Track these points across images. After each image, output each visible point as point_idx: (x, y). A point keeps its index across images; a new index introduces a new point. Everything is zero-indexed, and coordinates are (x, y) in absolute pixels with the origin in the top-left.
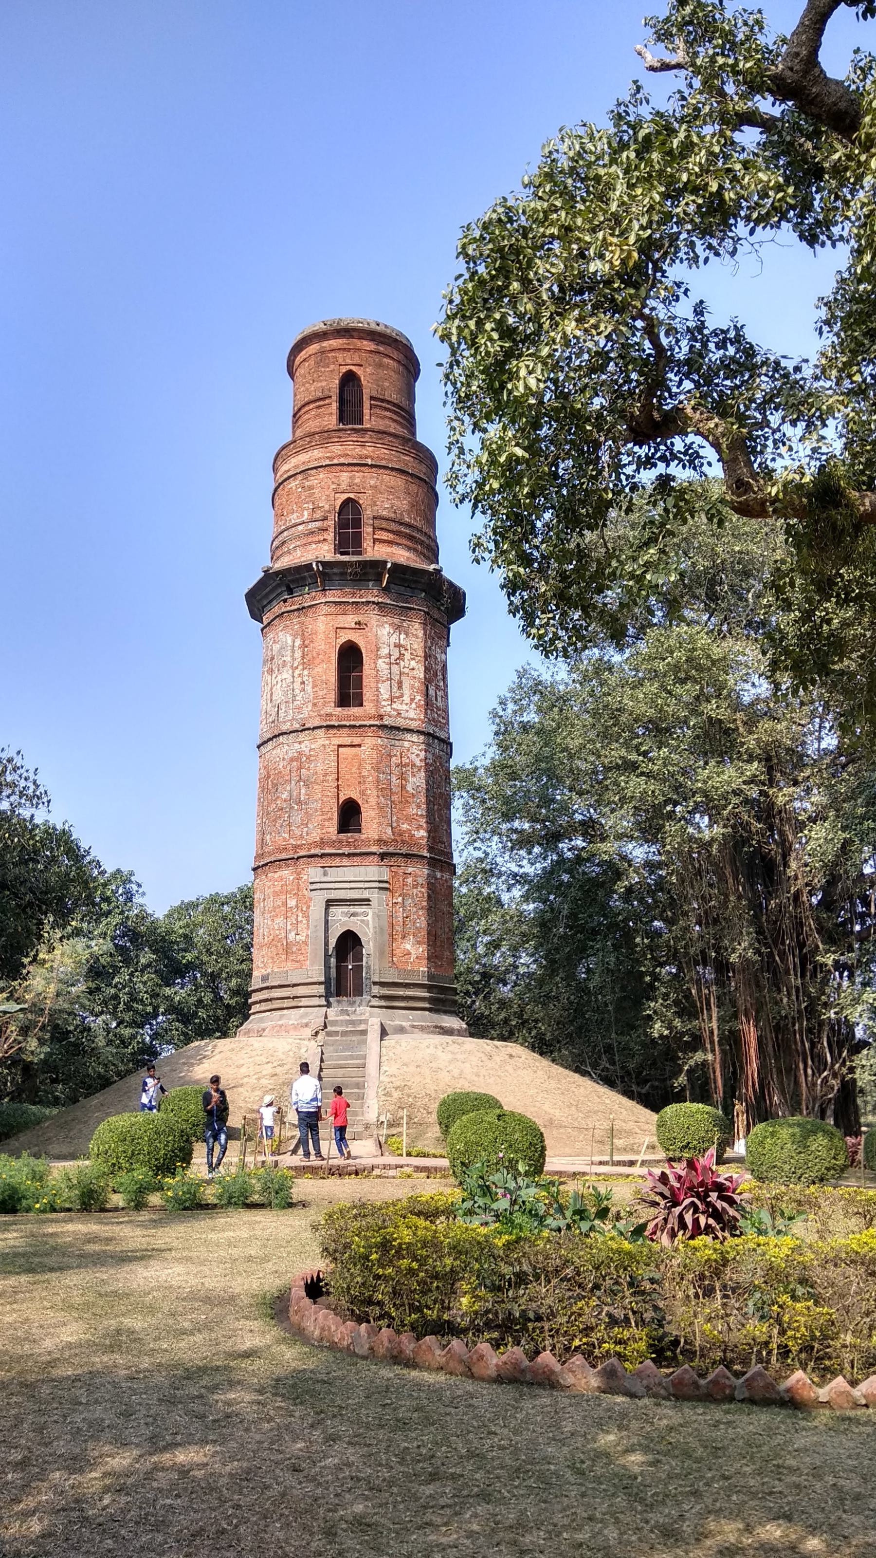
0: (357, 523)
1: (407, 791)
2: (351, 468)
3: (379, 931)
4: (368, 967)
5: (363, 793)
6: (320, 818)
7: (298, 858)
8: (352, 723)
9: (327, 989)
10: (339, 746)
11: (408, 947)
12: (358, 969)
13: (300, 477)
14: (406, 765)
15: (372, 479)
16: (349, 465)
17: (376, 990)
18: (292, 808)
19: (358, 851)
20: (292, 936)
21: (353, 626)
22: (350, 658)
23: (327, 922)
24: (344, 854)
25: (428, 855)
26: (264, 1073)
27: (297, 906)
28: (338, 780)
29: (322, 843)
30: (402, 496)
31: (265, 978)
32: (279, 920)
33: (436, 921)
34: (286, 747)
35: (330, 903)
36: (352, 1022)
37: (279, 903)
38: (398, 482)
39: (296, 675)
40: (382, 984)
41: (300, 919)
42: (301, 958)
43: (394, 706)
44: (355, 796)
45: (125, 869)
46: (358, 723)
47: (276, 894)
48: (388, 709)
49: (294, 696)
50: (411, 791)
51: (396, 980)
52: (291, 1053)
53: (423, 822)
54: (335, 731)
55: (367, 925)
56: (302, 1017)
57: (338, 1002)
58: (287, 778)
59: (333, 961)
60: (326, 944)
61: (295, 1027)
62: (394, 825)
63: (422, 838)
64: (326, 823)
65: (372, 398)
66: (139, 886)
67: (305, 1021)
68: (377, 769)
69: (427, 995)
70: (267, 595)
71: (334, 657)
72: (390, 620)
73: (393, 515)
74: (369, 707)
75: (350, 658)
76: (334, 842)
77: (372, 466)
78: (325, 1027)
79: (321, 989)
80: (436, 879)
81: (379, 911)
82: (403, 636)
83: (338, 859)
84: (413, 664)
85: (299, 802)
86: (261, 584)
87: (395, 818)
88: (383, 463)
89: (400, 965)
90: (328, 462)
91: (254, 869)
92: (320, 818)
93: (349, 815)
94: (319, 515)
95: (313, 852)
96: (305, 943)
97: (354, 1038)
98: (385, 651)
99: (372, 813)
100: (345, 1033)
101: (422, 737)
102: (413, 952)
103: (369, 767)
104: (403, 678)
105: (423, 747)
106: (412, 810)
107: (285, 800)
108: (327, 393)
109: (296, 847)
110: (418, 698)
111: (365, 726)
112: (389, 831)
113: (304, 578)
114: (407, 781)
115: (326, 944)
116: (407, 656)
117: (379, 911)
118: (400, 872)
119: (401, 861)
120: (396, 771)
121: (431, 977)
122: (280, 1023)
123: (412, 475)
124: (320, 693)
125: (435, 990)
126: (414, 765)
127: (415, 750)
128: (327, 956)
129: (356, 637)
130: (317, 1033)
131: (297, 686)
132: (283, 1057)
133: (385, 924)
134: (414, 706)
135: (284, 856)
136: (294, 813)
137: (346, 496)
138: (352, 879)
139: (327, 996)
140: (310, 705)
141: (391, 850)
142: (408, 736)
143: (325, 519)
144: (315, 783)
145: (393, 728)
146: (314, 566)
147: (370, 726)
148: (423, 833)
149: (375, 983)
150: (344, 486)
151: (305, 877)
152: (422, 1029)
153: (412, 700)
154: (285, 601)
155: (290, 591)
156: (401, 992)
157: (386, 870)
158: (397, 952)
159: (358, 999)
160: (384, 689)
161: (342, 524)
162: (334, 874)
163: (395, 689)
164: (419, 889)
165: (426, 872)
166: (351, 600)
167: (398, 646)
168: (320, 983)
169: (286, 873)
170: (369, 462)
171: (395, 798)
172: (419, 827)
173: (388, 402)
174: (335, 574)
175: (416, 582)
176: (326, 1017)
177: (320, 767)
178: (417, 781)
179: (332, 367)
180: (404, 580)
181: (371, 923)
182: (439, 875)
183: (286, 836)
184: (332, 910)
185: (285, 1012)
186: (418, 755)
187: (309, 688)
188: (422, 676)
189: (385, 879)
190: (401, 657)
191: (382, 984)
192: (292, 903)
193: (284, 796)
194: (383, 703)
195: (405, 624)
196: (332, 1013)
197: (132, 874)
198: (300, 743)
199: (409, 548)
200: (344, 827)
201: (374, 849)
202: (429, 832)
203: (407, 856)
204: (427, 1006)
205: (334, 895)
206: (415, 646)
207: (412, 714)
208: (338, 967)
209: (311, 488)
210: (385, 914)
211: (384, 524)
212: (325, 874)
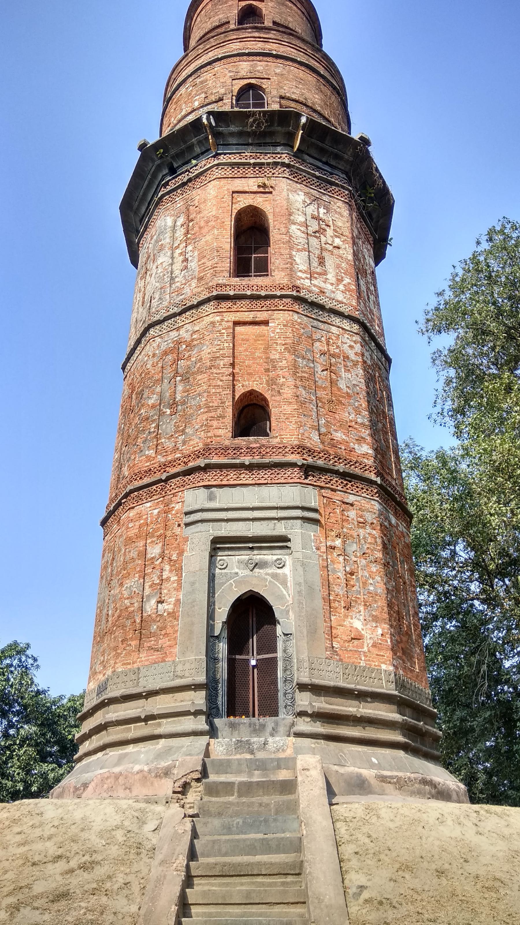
1: (339, 389)
2: (251, 58)
3: (306, 591)
4: (288, 659)
5: (272, 382)
6: (205, 416)
7: (168, 478)
9: (211, 699)
10: (236, 323)
11: (358, 624)
12: (268, 667)
13: (191, 79)
14: (333, 356)
15: (277, 68)
17: (305, 701)
18: (161, 414)
19: (267, 460)
20: (150, 606)
21: (255, 189)
22: (251, 235)
23: (212, 578)
24: (242, 466)
25: (378, 480)
26: (39, 888)
27: (162, 555)
28: (233, 365)
29: (207, 450)
31: (102, 688)
32: (132, 583)
33: (397, 589)
34: (158, 340)
35: (218, 544)
36: (262, 766)
37: (134, 554)
39: (176, 254)
40: (317, 690)
41: (165, 575)
42: (164, 642)
44: (258, 385)
45: (22, 641)
47: (130, 541)
48: (307, 283)
49: (172, 279)
50: (345, 389)
51: (341, 684)
52: (119, 836)
53: (366, 433)
54: (229, 304)
55: (284, 583)
56: (159, 756)
57: (233, 726)
58: (157, 377)
59: (222, 647)
60: (211, 616)
61: (144, 778)
62: (323, 430)
63: (365, 455)
64: (215, 423)
66: (35, 660)
67: (164, 764)
68: (293, 349)
69: (396, 717)
70: (145, 194)
71: (229, 224)
72: (307, 190)
75: (251, 235)
76: (227, 448)
78: (204, 773)
79: (199, 699)
80: (390, 524)
81: (305, 557)
82: (322, 211)
83: (232, 474)
84: (337, 242)
85: (174, 404)
86: (139, 174)
87: (323, 421)
89: (346, 656)
91: (104, 523)
92: (205, 416)
93: (251, 415)
94: (213, 98)
95: (191, 465)
96: (173, 615)
97: (265, 799)
99: (288, 409)
100: (247, 789)
101: (356, 327)
102: (366, 634)
104: (325, 254)
105: (357, 338)
106: (347, 414)
107: (153, 406)
109: (164, 466)
110: (347, 280)
111: (274, 297)
112: (315, 437)
113: (190, 148)
114: (339, 376)
115: (211, 616)
116: (330, 232)
117: (305, 557)
118: (338, 496)
119: (336, 482)
121: (400, 685)
122: (117, 770)
124: (209, 264)
125: (408, 711)
128: (211, 639)
129: (259, 201)
130: (185, 787)
131: (178, 266)
132: (97, 842)
133: (317, 580)
134: (341, 287)
135: (146, 480)
136: (165, 419)
137: (246, 82)
138: (257, 504)
139: (211, 713)
140: (194, 283)
141: (320, 463)
142: (337, 321)
143: (221, 99)
144: (200, 372)
145: (314, 305)
146: (205, 121)
147: (282, 297)
148: (365, 449)
149: (302, 687)
150: (243, 73)
151: (178, 507)
152: (400, 785)
153: (340, 281)
154: (167, 184)
156: (351, 708)
158: (338, 631)
159: (269, 721)
160: (300, 260)
162: (225, 498)
163: (315, 263)
164: (369, 530)
165: (377, 506)
168: (197, 687)
169: (149, 509)
170: (274, 53)
171: (320, 393)
172: (360, 440)
174: (232, 134)
175: (337, 157)
176: (207, 754)
177: (206, 351)
178: (352, 379)
180: (322, 151)
181: (290, 579)
182: (393, 521)
183: (151, 453)
184: (222, 557)
185: (131, 749)
186: (351, 347)
187: (193, 265)
188: (350, 257)
189: (313, 504)
190: (320, 231)
191: (317, 690)
192: (154, 551)
193: (151, 402)
194: (300, 274)
195: (325, 198)
196: (220, 748)
197: (28, 646)
200: (242, 267)
202: (376, 450)
203: (345, 476)
204: (398, 737)
206: (340, 224)
207: (340, 296)
208: (231, 662)
209: (201, 83)
210: (315, 562)
212: (211, 498)
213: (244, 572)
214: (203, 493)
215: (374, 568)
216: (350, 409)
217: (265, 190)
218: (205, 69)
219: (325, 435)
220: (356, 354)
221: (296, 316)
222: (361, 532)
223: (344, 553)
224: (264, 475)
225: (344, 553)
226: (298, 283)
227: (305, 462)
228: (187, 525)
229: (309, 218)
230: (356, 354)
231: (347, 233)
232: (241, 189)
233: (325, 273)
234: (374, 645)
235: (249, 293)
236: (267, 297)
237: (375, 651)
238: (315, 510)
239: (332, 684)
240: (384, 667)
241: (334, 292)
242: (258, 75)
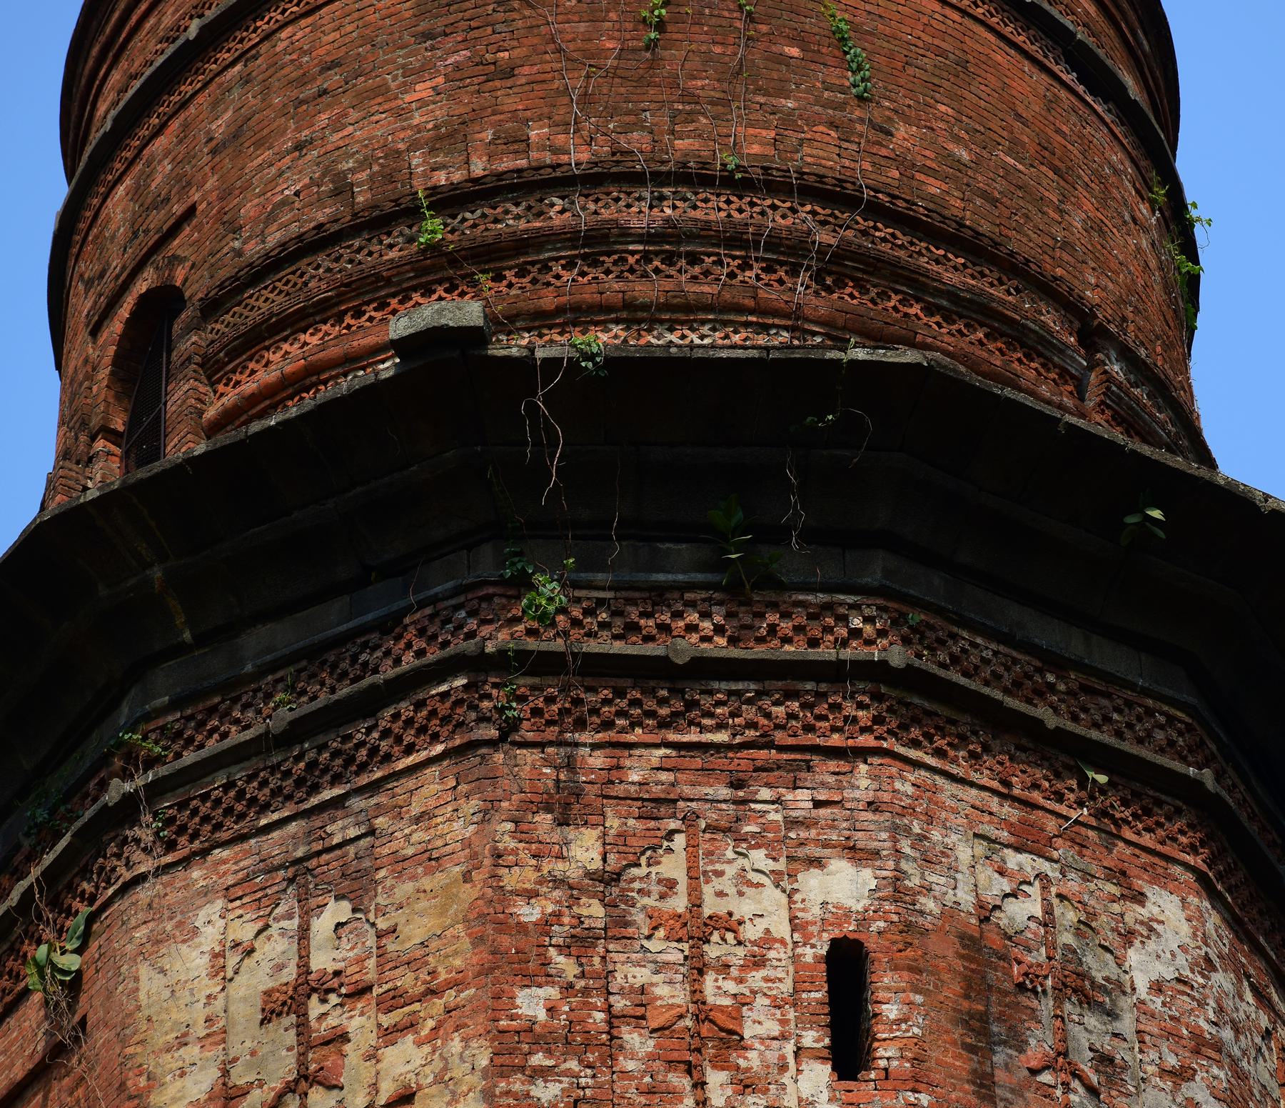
137: (124, 312)
167: (285, 1004)
211: (266, 302)
229: (245, 1035)
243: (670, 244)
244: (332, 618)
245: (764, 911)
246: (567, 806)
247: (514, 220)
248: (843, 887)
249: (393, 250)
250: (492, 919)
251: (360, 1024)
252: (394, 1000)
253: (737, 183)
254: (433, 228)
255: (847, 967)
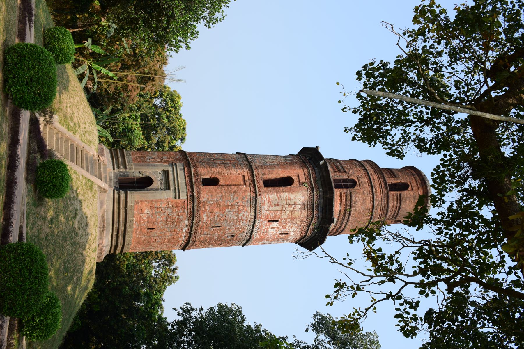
0: (346, 187)
1: (225, 210)
7: (188, 160)
8: (256, 181)
10: (244, 176)
11: (146, 211)
14: (239, 209)
15: (367, 191)
16: (371, 182)
24: (192, 177)
30: (363, 207)
35: (166, 173)
38: (368, 205)
43: (266, 202)
46: (256, 183)
48: (265, 199)
65: (400, 194)
73: (353, 202)
74: (266, 189)
76: (197, 172)
77: (373, 192)
80: (182, 228)
82: (300, 206)
84: (288, 212)
88: (375, 197)
90: (369, 173)
98: (292, 196)
101: (253, 218)
103: (236, 189)
108: (397, 176)
110: (272, 215)
112: (205, 200)
118: (185, 206)
120: (235, 203)
123: (372, 212)
126: (239, 212)
127: (246, 214)
133: (157, 198)
134: (268, 212)
137: (357, 181)
141: (196, 201)
142: (253, 210)
145: (256, 200)
150: (361, 179)
155: (310, 159)
156: (122, 206)
157: (186, 198)
161: (344, 180)
162: (181, 174)
163: (274, 203)
166: (312, 180)
170: (374, 190)
172: (208, 216)
173: (400, 203)
174: (322, 173)
179: (408, 178)
182: (184, 230)
186: (244, 215)
189: (181, 197)
198: (243, 161)
199: (340, 211)
201: (195, 190)
203: (193, 209)
205: (170, 173)
206: (296, 213)
207: (263, 212)
211: (349, 198)
212: (181, 169)
213: (159, 179)
214: (182, 168)
215: (164, 218)
216: (219, 213)
217: (301, 184)
218: (363, 168)
219: (207, 203)
220: (241, 217)
221: (249, 194)
222: (175, 214)
223: (167, 208)
224: (188, 184)
225: (167, 208)
226: (263, 195)
227: (195, 194)
228: (172, 164)
229: (294, 200)
230: (241, 217)
231: (293, 216)
232: (300, 177)
233: (272, 206)
234: (140, 216)
235: (255, 178)
236: (255, 185)
237: (139, 216)
238: (179, 198)
239: (128, 200)
240: (135, 219)
241: (265, 209)
242: (361, 185)
243: (342, 223)
244: (321, 206)
245: (292, 230)
246: (302, 221)
247: (347, 214)
248: (292, 233)
249: (348, 207)
250: (295, 218)
251: (292, 209)
252: (292, 211)
253: (345, 226)
254: (348, 211)
255: (288, 234)
